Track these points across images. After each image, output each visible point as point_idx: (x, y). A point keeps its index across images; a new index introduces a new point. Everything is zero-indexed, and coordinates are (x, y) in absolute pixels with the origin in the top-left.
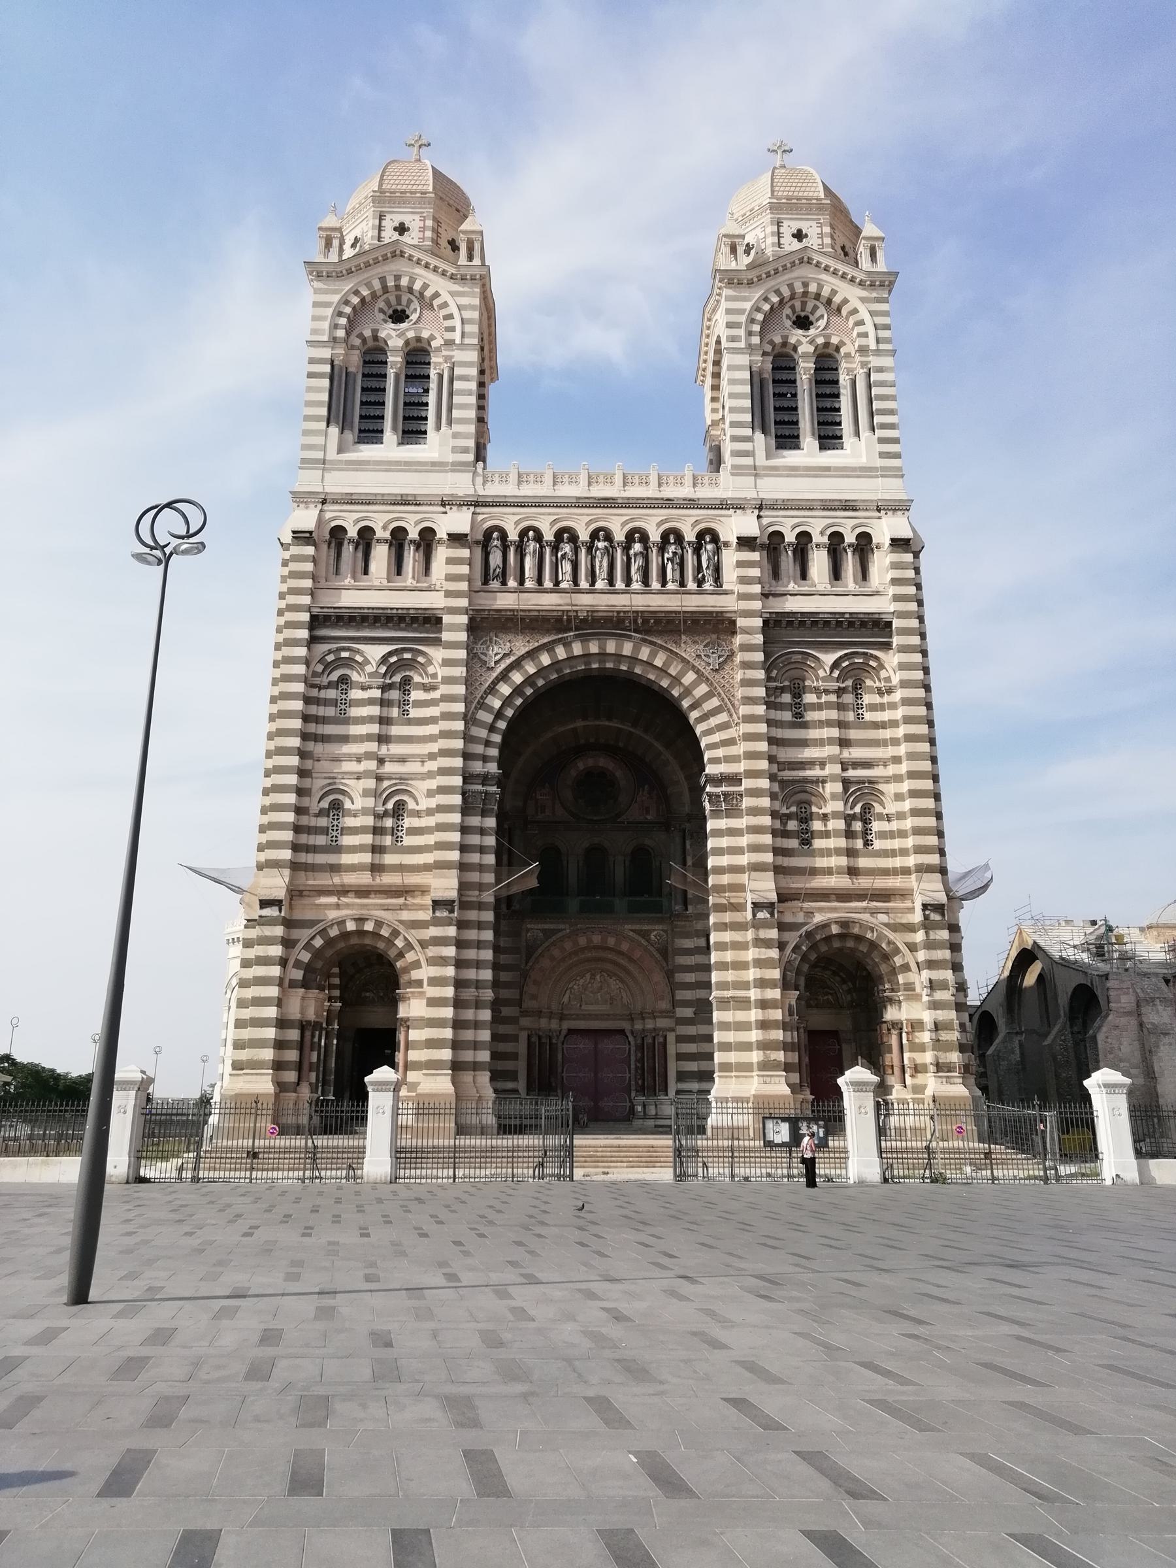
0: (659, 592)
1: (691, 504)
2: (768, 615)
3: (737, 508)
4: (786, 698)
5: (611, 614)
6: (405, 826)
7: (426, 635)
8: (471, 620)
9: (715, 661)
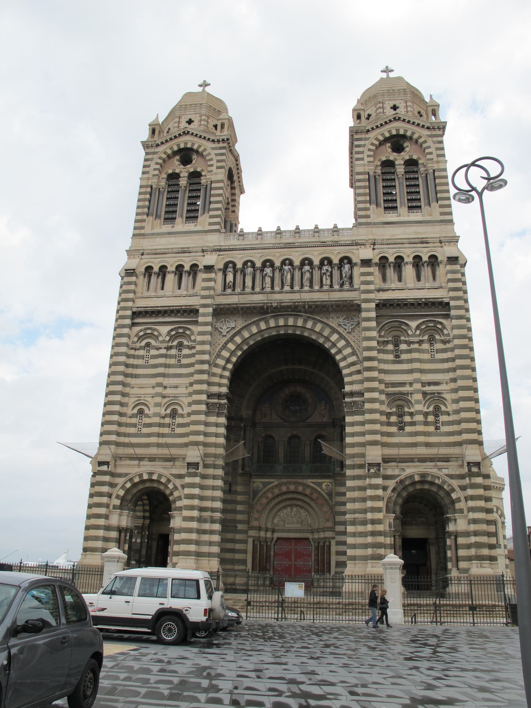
0: (318, 291)
1: (336, 244)
2: (378, 301)
3: (361, 245)
4: (390, 347)
5: (290, 304)
6: (176, 423)
7: (191, 319)
8: (214, 310)
9: (349, 327)
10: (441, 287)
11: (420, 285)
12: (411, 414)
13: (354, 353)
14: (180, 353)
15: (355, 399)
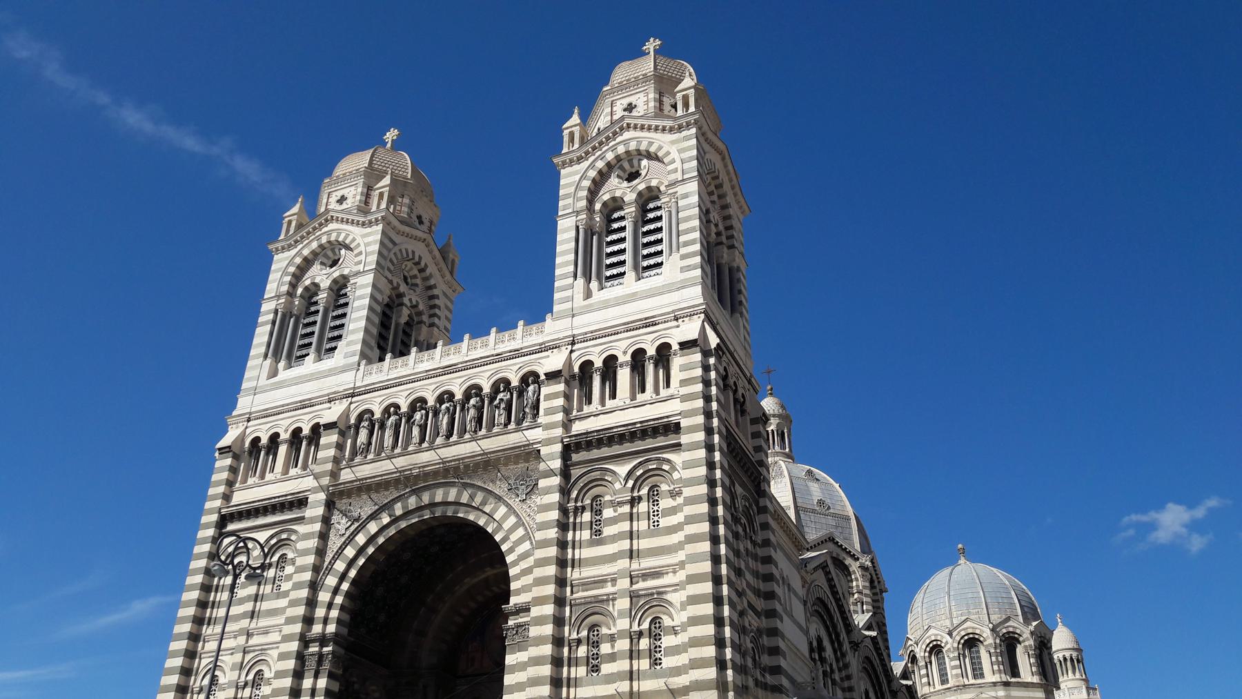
1: (517, 354)
10: (672, 397)
11: (641, 398)
12: (612, 639)
13: (527, 537)
14: (281, 574)
15: (521, 620)
